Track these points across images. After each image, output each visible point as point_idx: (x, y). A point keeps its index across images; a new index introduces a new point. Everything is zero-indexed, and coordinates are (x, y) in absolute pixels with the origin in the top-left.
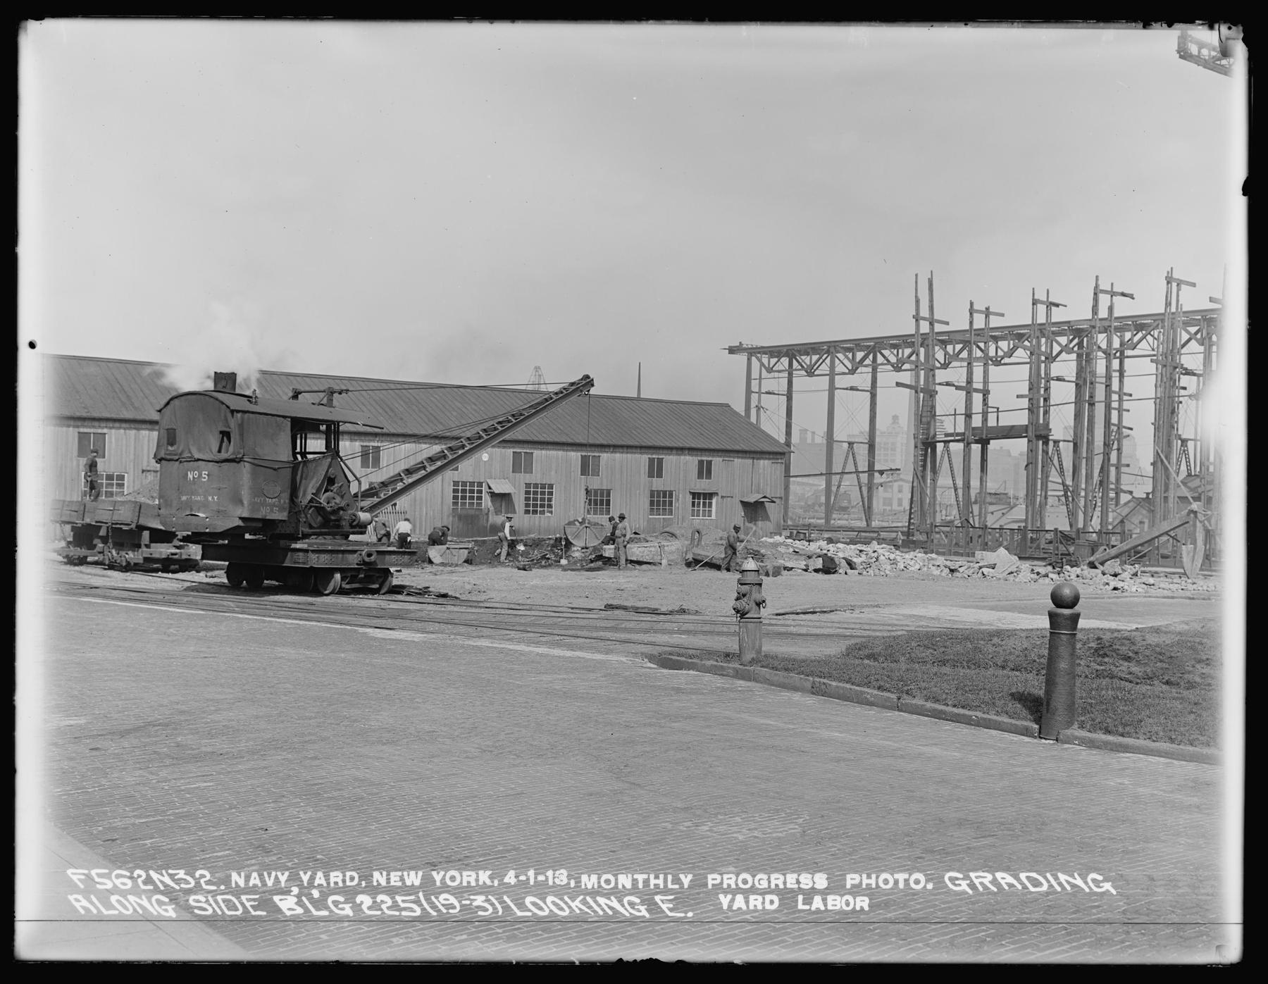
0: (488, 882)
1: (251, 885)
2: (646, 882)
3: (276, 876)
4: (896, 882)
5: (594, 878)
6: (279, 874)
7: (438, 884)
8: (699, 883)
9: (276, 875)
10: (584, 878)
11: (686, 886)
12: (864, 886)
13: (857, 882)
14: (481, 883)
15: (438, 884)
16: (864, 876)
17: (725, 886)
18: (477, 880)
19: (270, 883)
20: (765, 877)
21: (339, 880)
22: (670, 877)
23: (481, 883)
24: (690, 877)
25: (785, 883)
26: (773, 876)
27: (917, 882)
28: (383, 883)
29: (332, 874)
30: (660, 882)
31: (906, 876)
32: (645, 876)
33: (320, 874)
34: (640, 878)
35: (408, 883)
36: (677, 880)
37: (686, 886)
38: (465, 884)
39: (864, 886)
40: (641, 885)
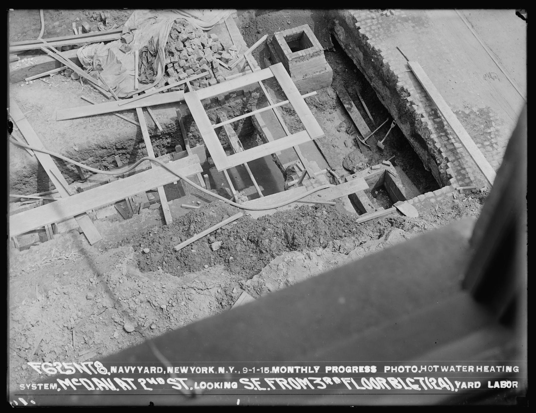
0: (213, 372)
1: (119, 372)
2: (300, 370)
3: (130, 368)
4: (406, 369)
5: (278, 368)
6: (131, 367)
7: (193, 372)
8: (322, 370)
9: (130, 368)
10: (273, 368)
11: (317, 372)
12: (392, 371)
13: (389, 369)
14: (210, 372)
15: (193, 372)
16: (392, 367)
17: (333, 372)
18: (208, 371)
19: (127, 371)
20: (350, 368)
21: (154, 370)
22: (310, 368)
23: (210, 372)
24: (318, 367)
25: (358, 370)
26: (353, 367)
27: (414, 369)
28: (172, 372)
29: (151, 368)
30: (306, 370)
31: (410, 367)
32: (299, 367)
33: (146, 368)
34: (297, 368)
35: (182, 372)
36: (313, 369)
37: (317, 372)
38: (203, 372)
39: (392, 371)
40: (297, 372)
